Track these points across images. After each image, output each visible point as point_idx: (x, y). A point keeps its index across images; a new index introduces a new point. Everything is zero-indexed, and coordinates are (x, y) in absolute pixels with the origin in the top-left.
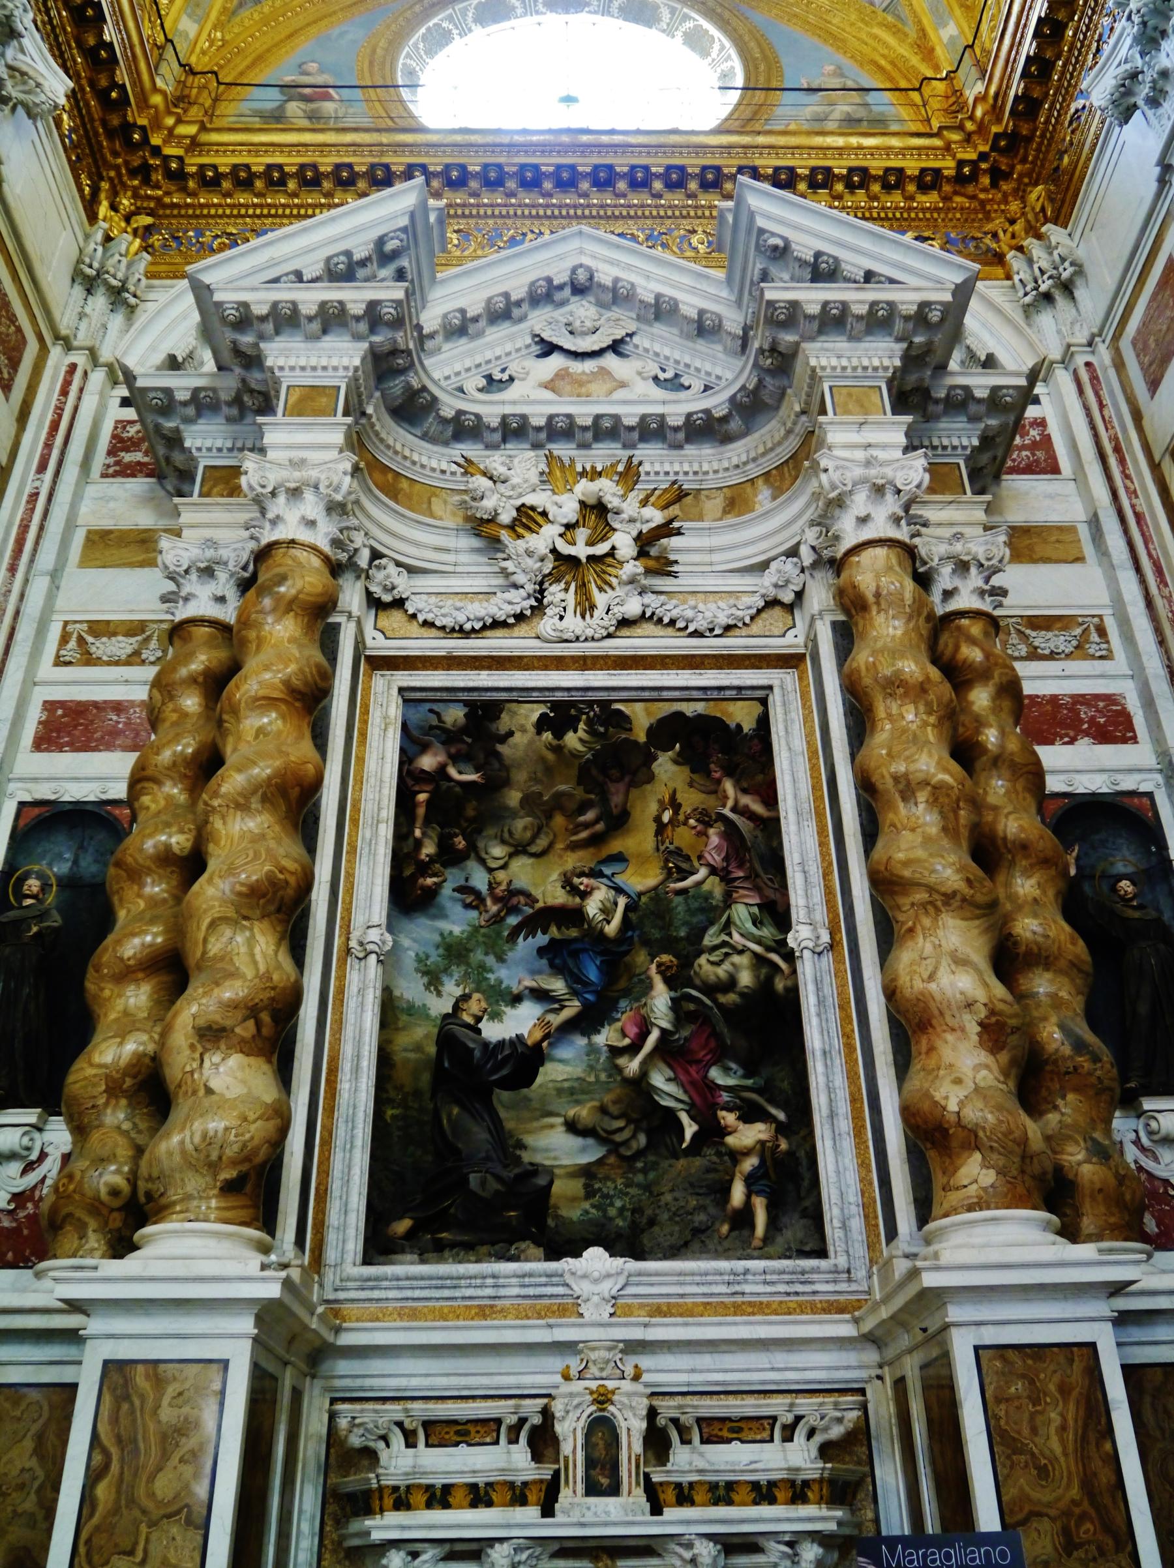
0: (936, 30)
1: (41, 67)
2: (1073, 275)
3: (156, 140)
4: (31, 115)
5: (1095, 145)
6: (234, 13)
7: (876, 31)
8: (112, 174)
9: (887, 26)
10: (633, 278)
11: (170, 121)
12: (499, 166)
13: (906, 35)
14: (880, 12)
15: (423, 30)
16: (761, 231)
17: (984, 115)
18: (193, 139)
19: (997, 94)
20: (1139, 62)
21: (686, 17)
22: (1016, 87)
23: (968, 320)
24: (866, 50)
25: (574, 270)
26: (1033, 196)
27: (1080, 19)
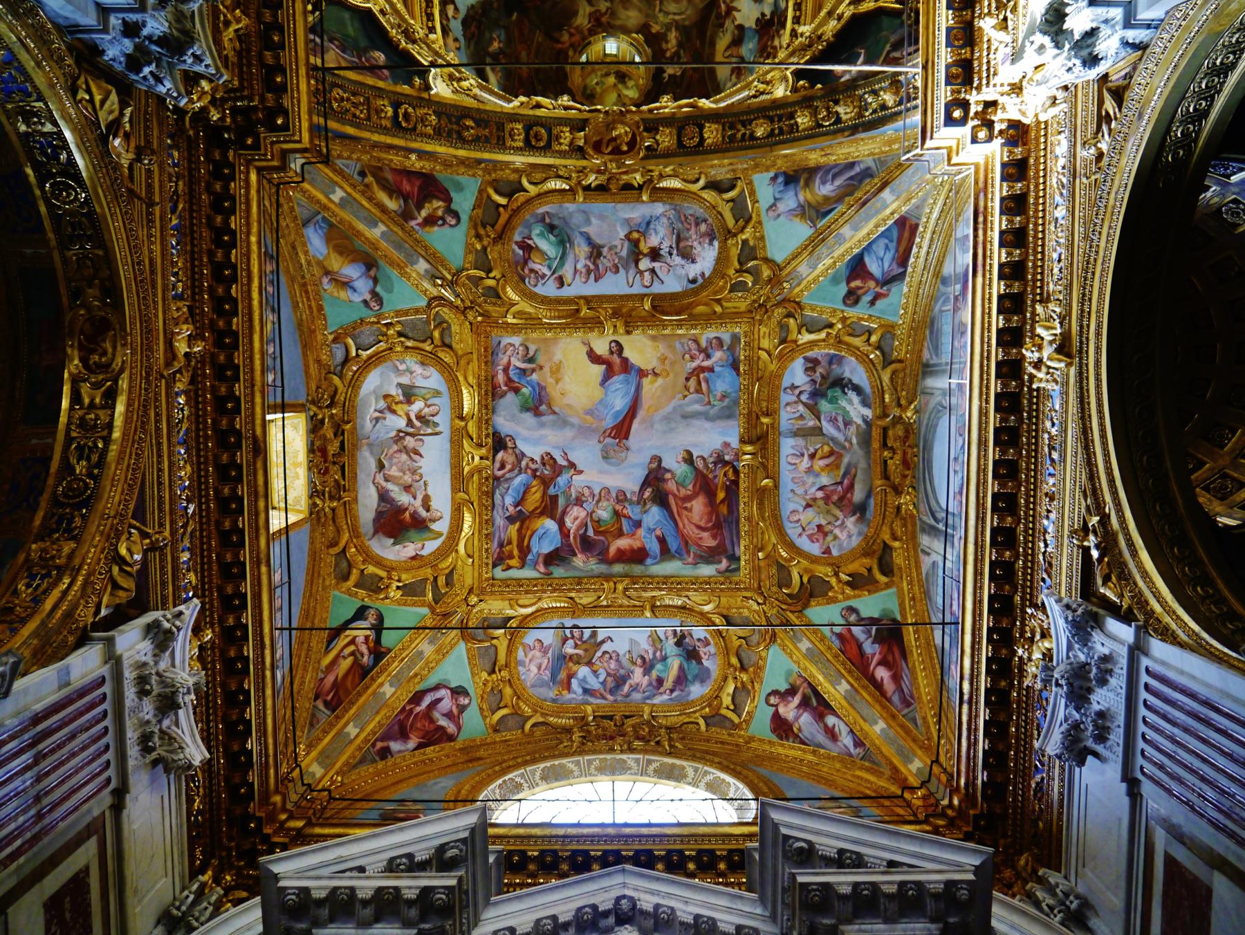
0: (905, 766)
1: (188, 739)
2: (1081, 906)
3: (268, 830)
4: (167, 771)
5: (1062, 801)
6: (355, 767)
7: (858, 773)
8: (224, 854)
9: (867, 770)
10: (672, 903)
11: (283, 817)
12: (555, 852)
13: (882, 773)
14: (858, 761)
15: (500, 781)
16: (786, 838)
17: (960, 802)
18: (299, 830)
19: (966, 784)
20: (1077, 716)
21: (706, 773)
22: (981, 777)
23: (994, 923)
24: (851, 785)
25: (618, 899)
26: (1022, 862)
27: (1018, 718)
